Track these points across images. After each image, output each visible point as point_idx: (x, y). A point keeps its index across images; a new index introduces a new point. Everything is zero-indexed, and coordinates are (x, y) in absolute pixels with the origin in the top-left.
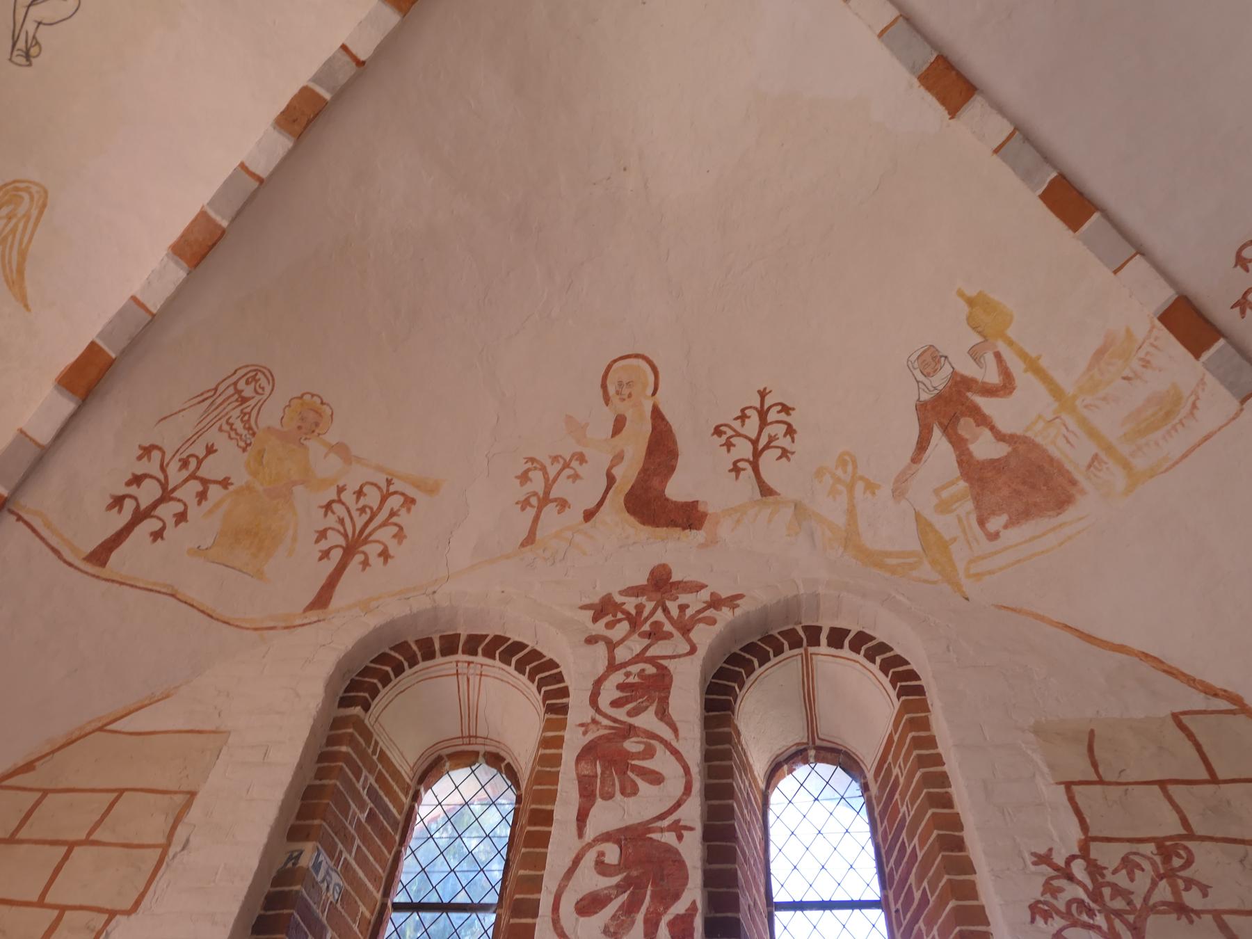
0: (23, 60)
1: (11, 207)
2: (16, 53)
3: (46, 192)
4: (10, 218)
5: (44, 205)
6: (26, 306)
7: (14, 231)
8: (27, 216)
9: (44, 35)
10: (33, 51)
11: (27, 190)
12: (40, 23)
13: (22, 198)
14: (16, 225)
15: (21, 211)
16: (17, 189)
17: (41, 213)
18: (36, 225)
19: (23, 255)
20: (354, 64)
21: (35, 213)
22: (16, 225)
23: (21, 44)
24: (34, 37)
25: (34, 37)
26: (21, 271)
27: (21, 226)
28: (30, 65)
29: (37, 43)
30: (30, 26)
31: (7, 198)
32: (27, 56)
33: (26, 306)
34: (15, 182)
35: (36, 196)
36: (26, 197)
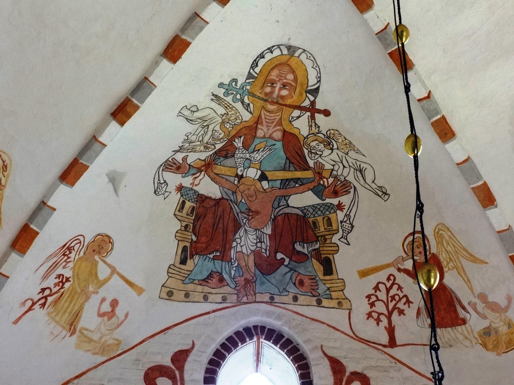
0: (386, 197)
1: (444, 240)
2: (383, 197)
3: (443, 224)
4: (448, 244)
5: (448, 229)
6: (486, 263)
7: (454, 246)
8: (450, 237)
9: (380, 182)
10: (384, 190)
11: (440, 230)
12: (373, 182)
13: (441, 234)
14: (453, 244)
15: (447, 238)
16: (438, 233)
17: (450, 232)
18: (455, 237)
19: (465, 250)
20: (428, 99)
21: (449, 234)
22: (453, 244)
23: (380, 193)
24: (378, 187)
25: (378, 187)
26: (471, 255)
27: (453, 242)
28: (389, 195)
29: (381, 187)
30: (374, 186)
31: (440, 239)
32: (385, 194)
33: (486, 263)
34: (434, 232)
35: (443, 228)
36: (441, 232)
